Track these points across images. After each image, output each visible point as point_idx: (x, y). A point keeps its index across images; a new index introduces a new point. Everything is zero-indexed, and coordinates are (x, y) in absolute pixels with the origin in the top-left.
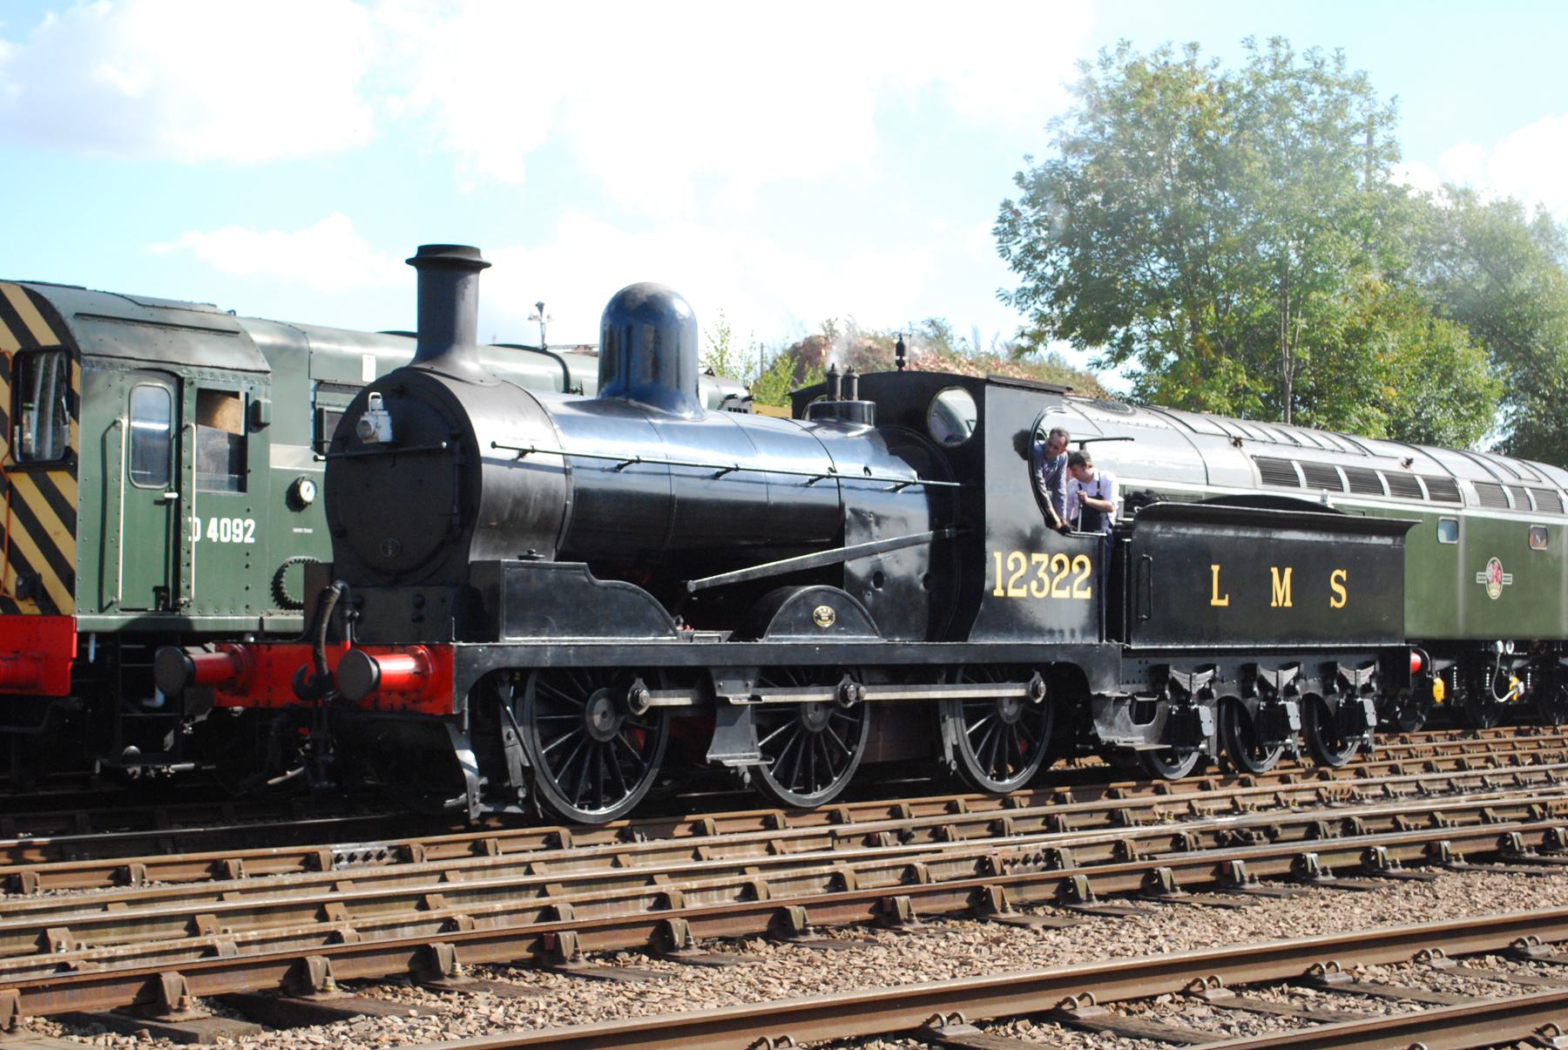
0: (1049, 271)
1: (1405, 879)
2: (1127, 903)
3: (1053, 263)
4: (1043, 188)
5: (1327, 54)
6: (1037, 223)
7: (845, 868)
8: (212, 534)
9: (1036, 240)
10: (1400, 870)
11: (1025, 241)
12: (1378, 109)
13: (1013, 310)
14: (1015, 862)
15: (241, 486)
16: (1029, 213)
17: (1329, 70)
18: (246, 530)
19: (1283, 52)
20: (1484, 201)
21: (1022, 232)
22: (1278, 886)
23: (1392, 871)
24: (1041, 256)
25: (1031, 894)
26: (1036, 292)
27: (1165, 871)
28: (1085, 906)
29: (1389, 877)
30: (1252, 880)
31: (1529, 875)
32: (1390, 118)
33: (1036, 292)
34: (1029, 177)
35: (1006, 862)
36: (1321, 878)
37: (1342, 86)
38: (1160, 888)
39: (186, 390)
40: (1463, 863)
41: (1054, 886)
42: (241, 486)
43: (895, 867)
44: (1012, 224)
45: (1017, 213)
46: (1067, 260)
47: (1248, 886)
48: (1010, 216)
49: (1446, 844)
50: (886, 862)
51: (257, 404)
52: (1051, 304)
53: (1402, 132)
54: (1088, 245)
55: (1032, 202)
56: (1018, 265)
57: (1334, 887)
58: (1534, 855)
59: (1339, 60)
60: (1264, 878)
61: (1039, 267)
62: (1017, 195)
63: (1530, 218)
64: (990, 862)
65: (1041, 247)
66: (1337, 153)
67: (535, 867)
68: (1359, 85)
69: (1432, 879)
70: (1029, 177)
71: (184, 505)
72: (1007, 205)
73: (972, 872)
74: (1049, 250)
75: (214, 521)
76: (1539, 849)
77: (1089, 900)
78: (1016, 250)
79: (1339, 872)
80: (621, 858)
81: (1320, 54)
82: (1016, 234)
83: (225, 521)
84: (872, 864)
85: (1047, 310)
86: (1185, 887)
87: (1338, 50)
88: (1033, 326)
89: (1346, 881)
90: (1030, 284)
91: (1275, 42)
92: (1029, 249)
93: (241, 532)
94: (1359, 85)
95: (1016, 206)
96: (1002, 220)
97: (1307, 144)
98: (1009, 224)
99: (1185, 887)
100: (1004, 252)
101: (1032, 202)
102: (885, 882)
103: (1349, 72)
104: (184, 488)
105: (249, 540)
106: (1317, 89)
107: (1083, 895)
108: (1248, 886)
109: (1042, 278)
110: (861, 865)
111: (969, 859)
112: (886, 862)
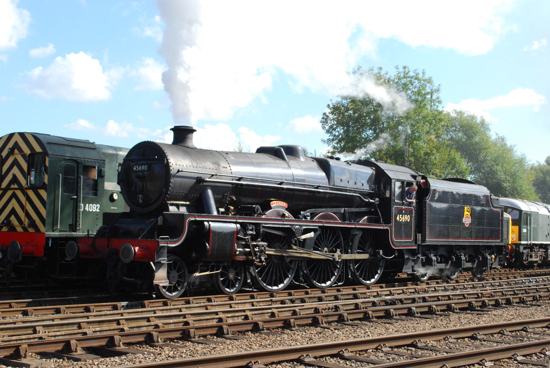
0: (337, 134)
1: (441, 315)
2: (359, 322)
3: (338, 131)
4: (336, 109)
5: (420, 71)
6: (333, 119)
7: (275, 311)
8: (87, 209)
9: (333, 125)
10: (440, 313)
11: (330, 125)
12: (435, 88)
13: (326, 145)
14: (326, 309)
15: (96, 194)
16: (331, 116)
17: (420, 76)
18: (97, 208)
19: (407, 70)
20: (465, 115)
21: (329, 122)
22: (403, 317)
23: (437, 313)
24: (334, 129)
25: (330, 319)
26: (333, 140)
27: (370, 312)
28: (347, 323)
29: (436, 315)
30: (396, 315)
31: (478, 314)
32: (438, 90)
33: (333, 140)
34: (331, 106)
35: (323, 309)
36: (416, 315)
37: (424, 81)
38: (369, 317)
39: (80, 166)
40: (458, 311)
41: (337, 317)
42: (96, 194)
43: (290, 311)
44: (326, 119)
45: (328, 116)
46: (342, 131)
47: (395, 317)
48: (325, 117)
49: (453, 305)
50: (287, 309)
51: (101, 170)
52: (337, 143)
53: (442, 95)
54: (348, 126)
55: (332, 113)
56: (328, 132)
57: (420, 317)
58: (479, 308)
59: (424, 73)
60: (399, 315)
61: (334, 132)
62: (328, 111)
63: (478, 121)
64: (318, 309)
65: (335, 127)
66: (422, 101)
67: (182, 310)
68: (430, 81)
69: (449, 315)
70: (331, 106)
71: (78, 200)
72: (324, 114)
73: (313, 312)
74: (337, 127)
75: (87, 205)
76: (480, 307)
77: (348, 321)
78: (327, 127)
79: (422, 313)
80: (208, 307)
81: (418, 71)
82: (327, 123)
83: (90, 205)
84: (283, 309)
85: (336, 145)
86: (376, 317)
87: (423, 70)
88: (331, 150)
89: (424, 316)
90: (331, 138)
91: (405, 68)
92: (331, 127)
93: (95, 208)
94: (430, 81)
95: (327, 114)
96: (323, 118)
97: (413, 97)
98: (325, 119)
99: (376, 317)
100: (324, 128)
101: (332, 113)
102: (287, 315)
103: (427, 77)
104: (79, 194)
105: (98, 210)
106: (416, 81)
107: (346, 319)
108: (395, 317)
109: (335, 136)
110: (280, 310)
111: (312, 308)
112: (287, 309)
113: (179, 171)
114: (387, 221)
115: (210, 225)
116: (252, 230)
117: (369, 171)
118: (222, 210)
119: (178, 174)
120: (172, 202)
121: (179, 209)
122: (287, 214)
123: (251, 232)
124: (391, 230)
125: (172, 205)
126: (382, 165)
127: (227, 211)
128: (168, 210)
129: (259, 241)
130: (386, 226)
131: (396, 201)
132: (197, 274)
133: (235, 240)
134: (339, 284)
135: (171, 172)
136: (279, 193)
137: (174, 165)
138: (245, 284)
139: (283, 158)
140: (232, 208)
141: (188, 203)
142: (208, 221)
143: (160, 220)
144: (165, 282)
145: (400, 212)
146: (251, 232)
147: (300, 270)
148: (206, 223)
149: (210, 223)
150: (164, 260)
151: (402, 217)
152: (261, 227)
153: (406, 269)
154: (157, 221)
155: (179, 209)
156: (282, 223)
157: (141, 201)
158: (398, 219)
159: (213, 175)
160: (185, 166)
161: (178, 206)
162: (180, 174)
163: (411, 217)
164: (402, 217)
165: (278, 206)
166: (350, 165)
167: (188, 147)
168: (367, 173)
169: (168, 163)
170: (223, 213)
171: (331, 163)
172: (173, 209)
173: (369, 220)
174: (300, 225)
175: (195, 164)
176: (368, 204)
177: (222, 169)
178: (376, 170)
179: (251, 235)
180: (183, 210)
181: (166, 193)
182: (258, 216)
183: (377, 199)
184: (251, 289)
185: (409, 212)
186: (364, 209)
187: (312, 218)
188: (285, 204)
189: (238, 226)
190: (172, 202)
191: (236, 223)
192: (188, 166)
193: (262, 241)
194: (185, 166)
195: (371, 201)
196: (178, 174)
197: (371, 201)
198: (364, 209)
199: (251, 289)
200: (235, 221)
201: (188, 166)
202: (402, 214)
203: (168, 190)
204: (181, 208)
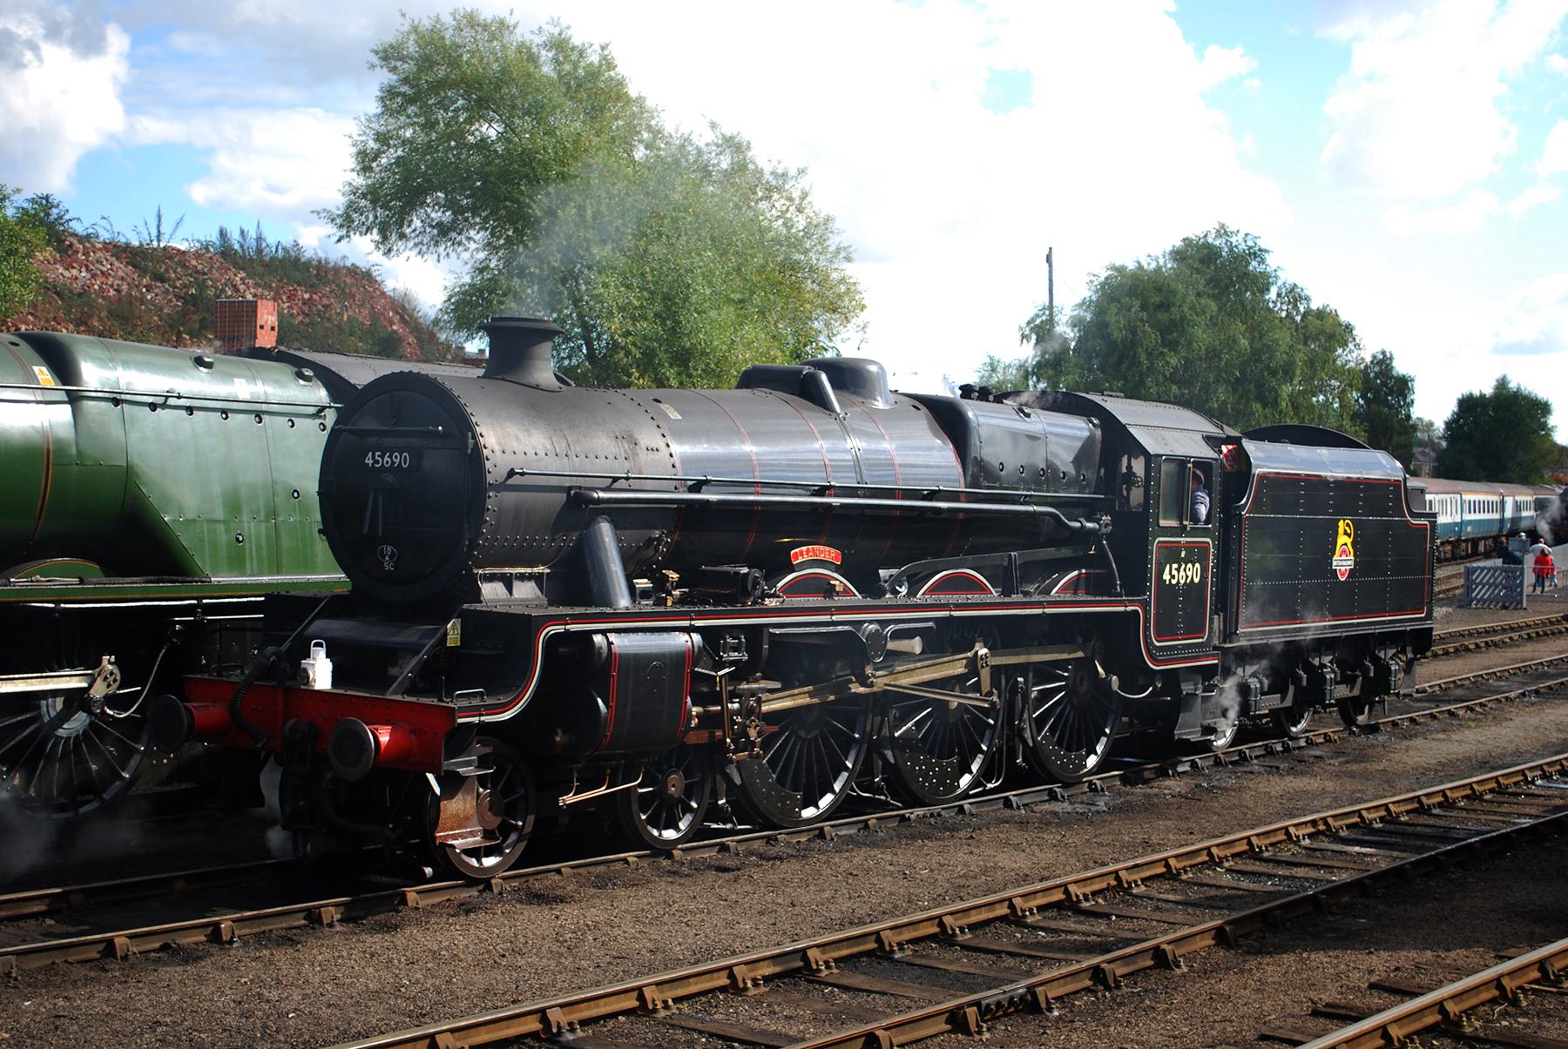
113: (512, 473)
114: (1136, 582)
115: (610, 644)
116: (735, 649)
117: (1077, 429)
118: (642, 583)
119: (510, 482)
120: (488, 571)
121: (510, 590)
122: (839, 581)
123: (734, 655)
124: (1147, 613)
125: (491, 578)
126: (1122, 409)
127: (661, 584)
128: (476, 595)
129: (756, 681)
130: (1132, 603)
131: (1163, 523)
132: (570, 799)
133: (687, 685)
134: (989, 786)
135: (490, 479)
136: (814, 520)
137: (498, 453)
138: (715, 814)
139: (822, 402)
140: (674, 576)
141: (540, 569)
142: (604, 632)
143: (453, 631)
144: (472, 834)
145: (1172, 555)
146: (734, 655)
147: (875, 756)
148: (598, 639)
149: (612, 637)
150: (468, 764)
151: (1178, 570)
152: (766, 639)
153: (1186, 726)
154: (446, 634)
155: (510, 590)
156: (826, 618)
157: (388, 566)
158: (1166, 577)
159: (615, 479)
160: (531, 453)
161: (508, 581)
162: (515, 480)
163: (1204, 570)
164: (1178, 570)
165: (814, 557)
166: (1028, 415)
167: (537, 387)
168: (1074, 438)
169: (477, 449)
170: (645, 594)
171: (970, 414)
172: (492, 592)
173: (1074, 586)
174: (879, 622)
175: (561, 446)
176: (1083, 536)
177: (644, 457)
178: (1103, 426)
179: (732, 663)
180: (525, 591)
181: (473, 544)
182: (754, 603)
183: (1106, 519)
184: (729, 826)
185: (1196, 555)
186: (1065, 552)
187: (912, 593)
188: (828, 553)
189: (696, 637)
190: (488, 571)
191: (688, 630)
192: (541, 453)
193: (764, 678)
194: (531, 453)
195: (1089, 525)
196: (510, 482)
197: (1089, 525)
198: (1065, 552)
199: (729, 826)
200: (686, 623)
201: (541, 453)
202: (1179, 561)
203: (479, 534)
204: (517, 585)
